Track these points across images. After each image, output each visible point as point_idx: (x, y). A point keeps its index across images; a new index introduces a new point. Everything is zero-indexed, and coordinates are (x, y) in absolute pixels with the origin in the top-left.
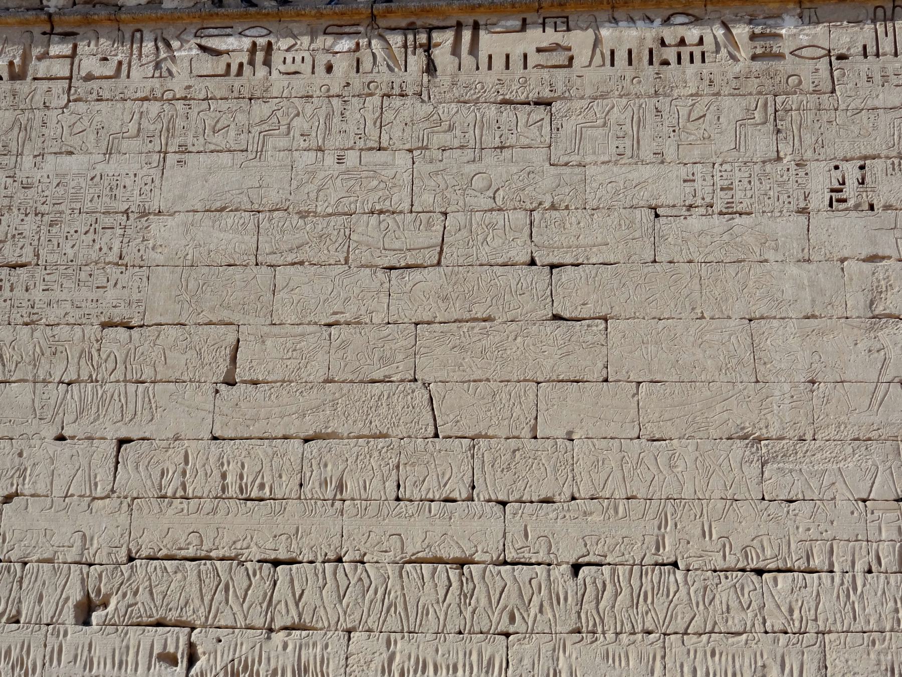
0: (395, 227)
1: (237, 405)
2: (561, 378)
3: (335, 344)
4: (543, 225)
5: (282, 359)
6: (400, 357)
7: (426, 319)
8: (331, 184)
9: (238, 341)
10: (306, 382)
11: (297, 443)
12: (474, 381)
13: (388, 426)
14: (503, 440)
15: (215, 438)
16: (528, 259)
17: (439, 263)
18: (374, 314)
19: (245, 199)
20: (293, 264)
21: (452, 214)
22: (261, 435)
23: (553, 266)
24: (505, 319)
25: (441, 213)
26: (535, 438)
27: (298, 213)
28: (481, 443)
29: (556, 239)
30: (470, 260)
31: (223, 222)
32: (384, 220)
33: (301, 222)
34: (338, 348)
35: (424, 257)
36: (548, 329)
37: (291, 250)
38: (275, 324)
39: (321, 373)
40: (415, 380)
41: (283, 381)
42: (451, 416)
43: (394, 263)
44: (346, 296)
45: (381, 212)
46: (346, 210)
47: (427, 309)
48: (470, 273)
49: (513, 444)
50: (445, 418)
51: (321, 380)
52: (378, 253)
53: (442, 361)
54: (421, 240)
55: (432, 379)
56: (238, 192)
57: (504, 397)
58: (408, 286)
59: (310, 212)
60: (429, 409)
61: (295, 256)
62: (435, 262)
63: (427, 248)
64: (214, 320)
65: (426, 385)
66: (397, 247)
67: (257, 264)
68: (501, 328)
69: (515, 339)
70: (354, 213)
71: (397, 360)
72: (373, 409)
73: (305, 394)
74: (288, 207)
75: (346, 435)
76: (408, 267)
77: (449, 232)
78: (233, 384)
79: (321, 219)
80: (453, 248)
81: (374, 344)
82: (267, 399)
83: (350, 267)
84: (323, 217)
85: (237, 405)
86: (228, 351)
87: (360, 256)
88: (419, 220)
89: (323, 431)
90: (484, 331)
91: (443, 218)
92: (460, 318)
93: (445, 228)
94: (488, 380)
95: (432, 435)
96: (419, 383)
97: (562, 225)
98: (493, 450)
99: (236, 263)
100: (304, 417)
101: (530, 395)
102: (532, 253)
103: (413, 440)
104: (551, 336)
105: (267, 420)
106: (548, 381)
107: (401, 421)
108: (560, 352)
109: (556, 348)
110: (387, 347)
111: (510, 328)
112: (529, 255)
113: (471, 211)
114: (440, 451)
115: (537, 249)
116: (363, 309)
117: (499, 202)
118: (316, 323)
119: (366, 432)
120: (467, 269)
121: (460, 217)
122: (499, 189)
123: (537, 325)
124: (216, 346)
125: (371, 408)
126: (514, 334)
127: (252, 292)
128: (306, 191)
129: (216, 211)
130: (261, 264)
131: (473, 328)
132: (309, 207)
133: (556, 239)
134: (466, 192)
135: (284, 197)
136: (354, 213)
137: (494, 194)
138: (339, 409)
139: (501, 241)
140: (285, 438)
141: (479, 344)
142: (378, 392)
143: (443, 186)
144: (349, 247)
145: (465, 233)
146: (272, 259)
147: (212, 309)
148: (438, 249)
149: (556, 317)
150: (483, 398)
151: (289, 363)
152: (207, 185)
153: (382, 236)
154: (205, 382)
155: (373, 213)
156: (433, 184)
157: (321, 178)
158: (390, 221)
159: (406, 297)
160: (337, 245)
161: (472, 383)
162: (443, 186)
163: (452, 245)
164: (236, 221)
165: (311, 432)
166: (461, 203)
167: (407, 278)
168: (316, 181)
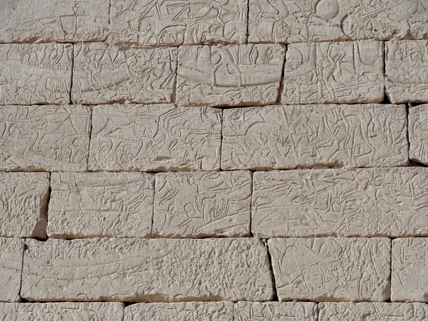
0: (228, 60)
1: (48, 262)
2: (418, 232)
3: (160, 194)
4: (398, 56)
5: (99, 211)
6: (233, 208)
7: (263, 165)
8: (155, 11)
9: (50, 190)
10: (126, 237)
11: (116, 306)
12: (319, 236)
13: (220, 287)
14: (351, 304)
15: (23, 300)
16: (380, 96)
17: (278, 101)
18: (203, 160)
19: (58, 28)
20: (112, 103)
21: (293, 45)
22: (75, 297)
23: (407, 104)
24: (354, 165)
25: (281, 43)
26: (389, 301)
27: (118, 44)
28: (326, 306)
29: (413, 73)
30: (314, 97)
31: (33, 55)
32: (215, 52)
33: (121, 55)
34: (163, 199)
35: (261, 94)
36: (403, 176)
37: (109, 87)
38: (91, 171)
39: (143, 226)
40: (251, 235)
41: (101, 236)
42: (292, 276)
43: (227, 101)
44: (172, 138)
45: (212, 43)
46: (172, 40)
47: (265, 154)
48: (314, 112)
49: (363, 308)
50: (285, 278)
51: (144, 234)
52: (208, 90)
53: (282, 213)
54: (257, 75)
55: (270, 234)
56: (49, 20)
57: (353, 254)
58: (242, 127)
59: (131, 44)
60: (266, 267)
61: (113, 93)
62: (274, 99)
63: (265, 84)
64: (23, 166)
65: (263, 241)
66: (230, 83)
67: (71, 103)
68: (349, 175)
69: (366, 188)
70: (182, 44)
71: (231, 212)
72: (203, 268)
73: (125, 250)
74: (106, 38)
75: (171, 297)
76: (242, 106)
77: (290, 66)
78: (44, 239)
79: (144, 51)
80: (295, 84)
81: (204, 194)
82: (82, 256)
83: (176, 106)
84: (147, 48)
85: (48, 262)
86: (38, 200)
87: (188, 93)
88: (255, 52)
89: (146, 293)
90: (330, 179)
91: (283, 50)
92: (302, 164)
93: (285, 60)
94: (334, 235)
95: (270, 297)
96: (256, 239)
97: (420, 56)
98: (340, 315)
99: (48, 101)
100: (124, 275)
101: (383, 252)
102: (385, 88)
103: (249, 303)
104: (407, 184)
105: (82, 281)
106: (403, 236)
107: (235, 282)
108: (417, 202)
109: (413, 198)
110: (218, 197)
111: (360, 176)
112: (382, 91)
113: (315, 41)
114: (279, 316)
115: (391, 84)
116: (192, 154)
117: (347, 31)
118: (137, 170)
119: (194, 294)
120: (311, 108)
121: (303, 47)
122: (346, 16)
123: (391, 172)
124: (25, 196)
125: (200, 266)
126: (364, 182)
127: (66, 134)
128: (127, 19)
129: (25, 42)
130: (76, 102)
131: (317, 175)
132: (131, 37)
133: (413, 73)
134: (310, 20)
135: (101, 26)
136: (182, 44)
137: (342, 22)
138: (164, 268)
139: (349, 75)
140: (103, 300)
141: (324, 194)
142: (208, 249)
143: (283, 12)
144: (175, 82)
145: (308, 66)
146: (88, 97)
147: (21, 154)
148: (277, 85)
149: (413, 163)
150: (329, 255)
151: (107, 214)
152: (14, 13)
153: (213, 70)
154: (12, 236)
155: (202, 44)
156: (272, 10)
157: (144, 4)
158: (222, 52)
159: (240, 140)
160: (162, 80)
161: (316, 239)
162: (283, 12)
163: (293, 80)
164: (48, 54)
165: (132, 294)
166: (304, 32)
167: (241, 118)
168: (137, 8)
